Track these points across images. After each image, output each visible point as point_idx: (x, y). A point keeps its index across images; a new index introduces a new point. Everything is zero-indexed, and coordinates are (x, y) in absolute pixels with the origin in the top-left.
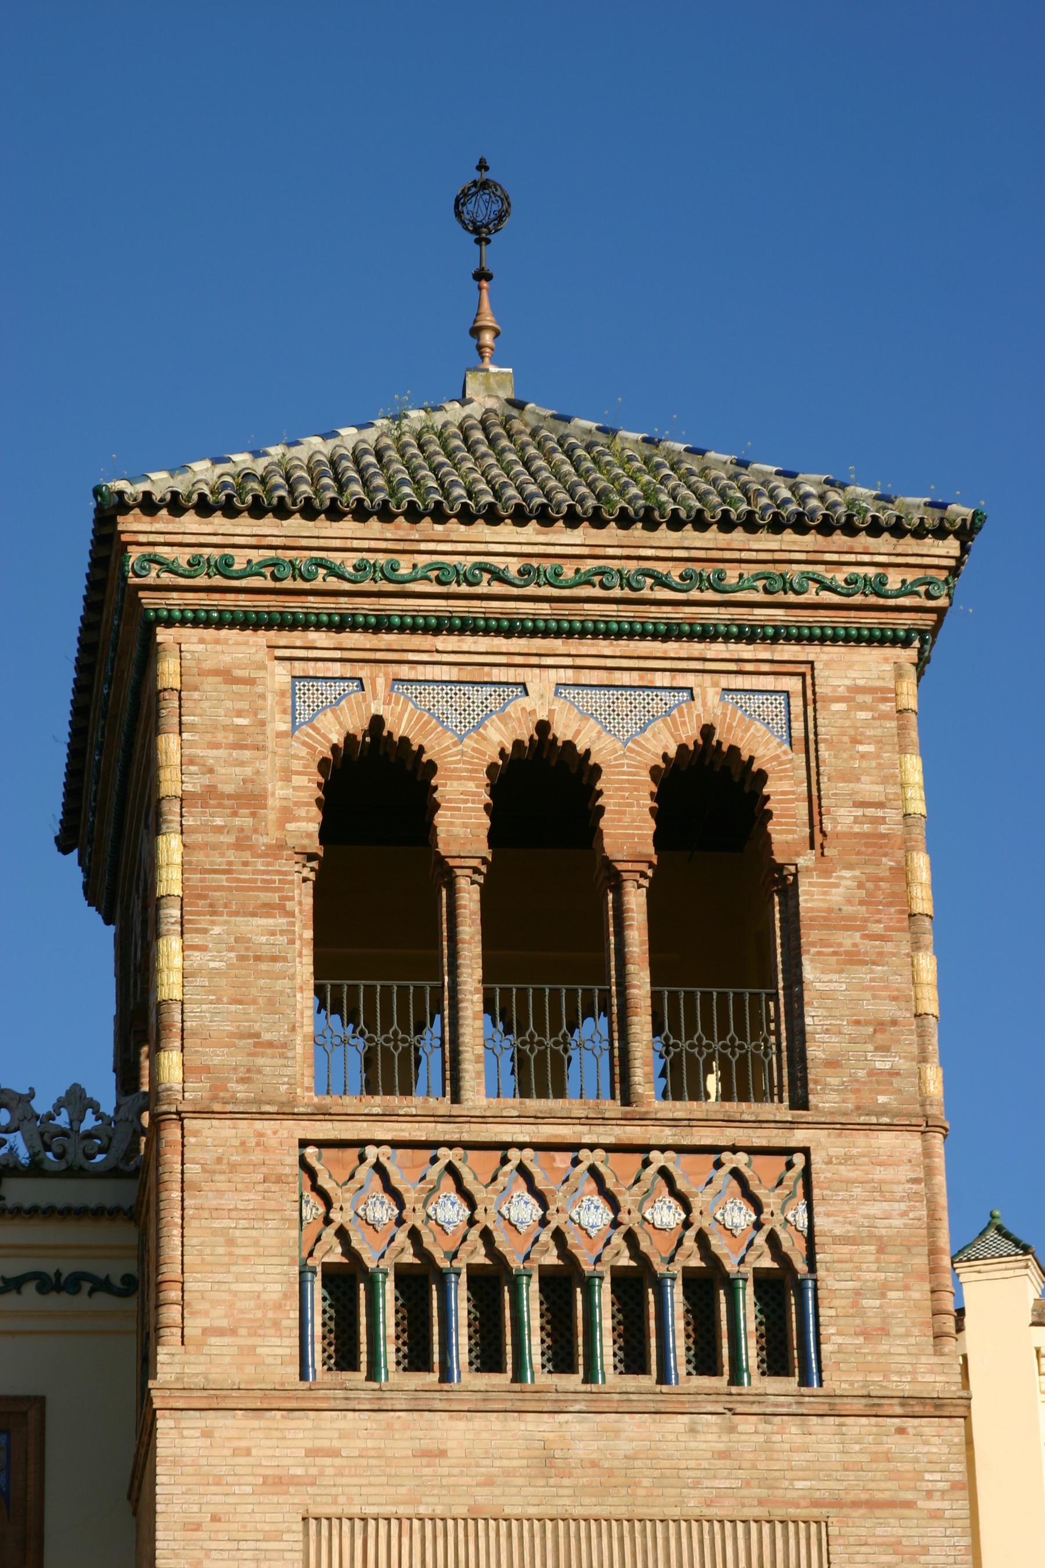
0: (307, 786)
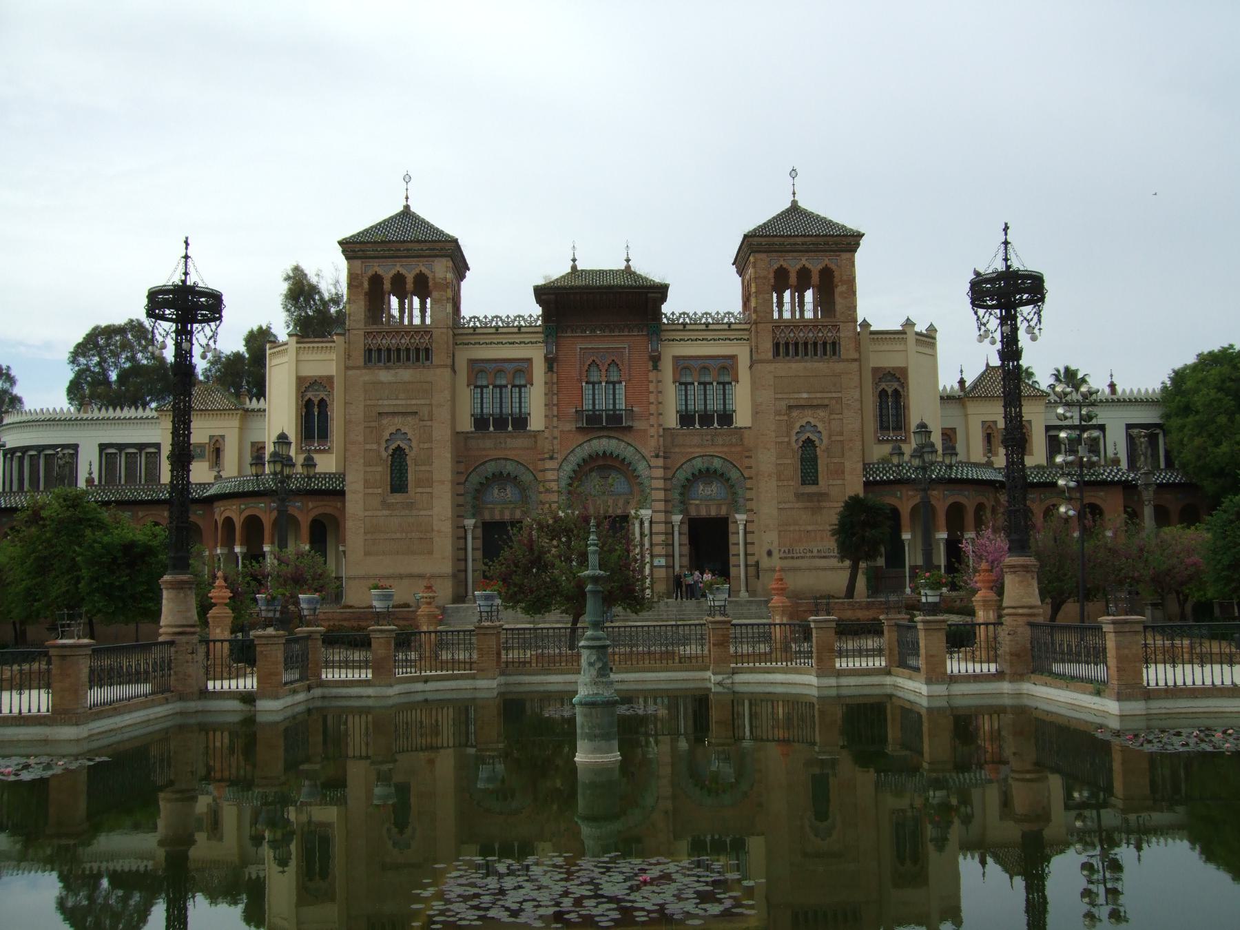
0: (772, 275)
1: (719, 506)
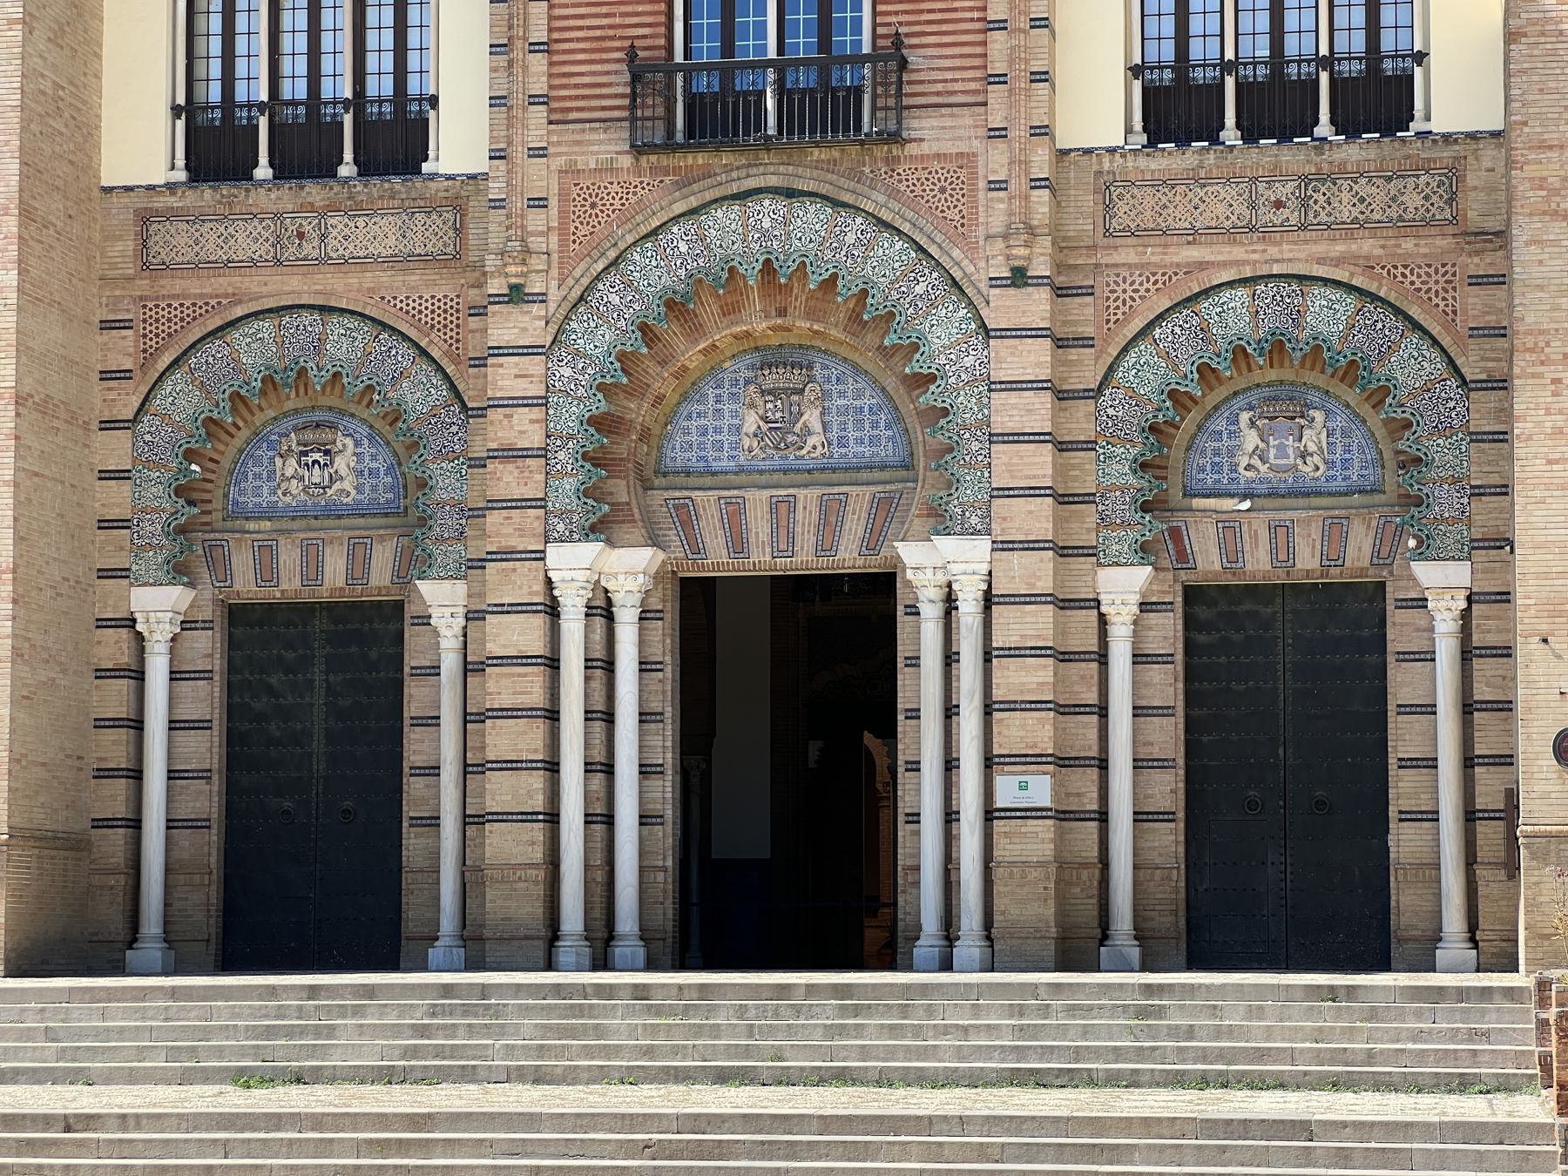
1: (1335, 532)
